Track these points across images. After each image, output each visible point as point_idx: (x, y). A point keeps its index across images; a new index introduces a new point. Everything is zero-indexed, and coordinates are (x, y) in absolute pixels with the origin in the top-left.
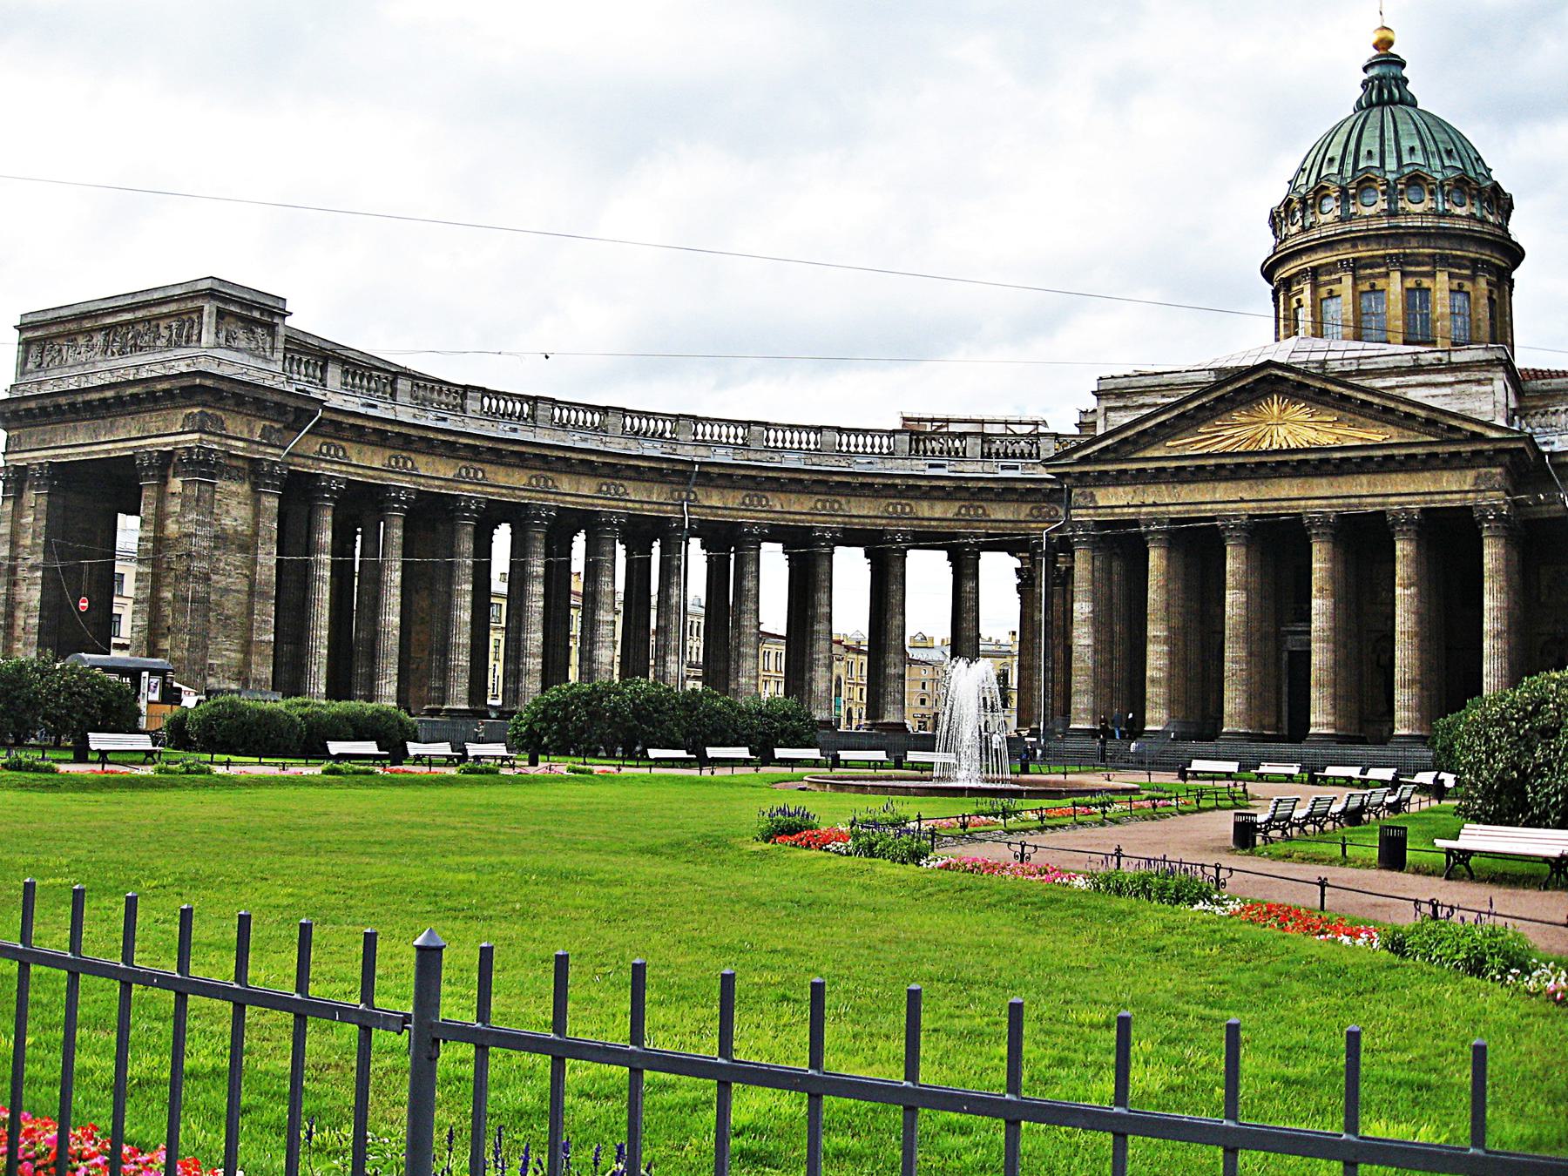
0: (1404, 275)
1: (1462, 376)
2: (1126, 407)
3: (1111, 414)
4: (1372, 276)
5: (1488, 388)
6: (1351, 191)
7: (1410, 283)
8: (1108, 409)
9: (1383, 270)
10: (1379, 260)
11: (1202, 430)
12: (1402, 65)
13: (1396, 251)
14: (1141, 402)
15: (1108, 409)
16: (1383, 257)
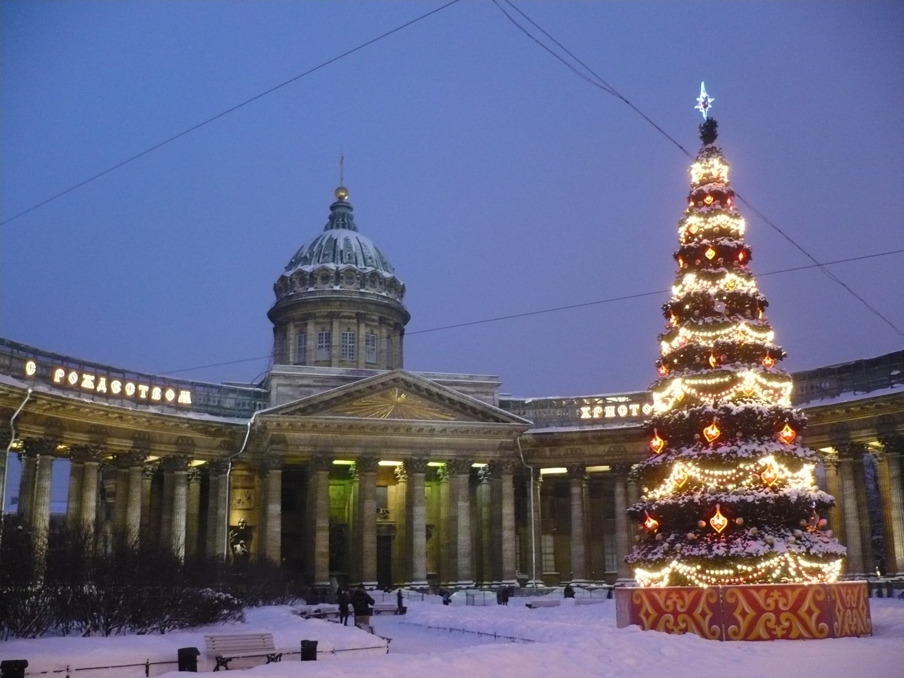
0: (366, 325)
1: (479, 389)
2: (290, 385)
3: (280, 389)
4: (349, 323)
5: (491, 397)
6: (342, 275)
7: (368, 330)
8: (279, 385)
9: (355, 321)
10: (354, 315)
11: (354, 404)
12: (351, 209)
13: (363, 312)
14: (300, 383)
15: (279, 385)
16: (357, 314)
